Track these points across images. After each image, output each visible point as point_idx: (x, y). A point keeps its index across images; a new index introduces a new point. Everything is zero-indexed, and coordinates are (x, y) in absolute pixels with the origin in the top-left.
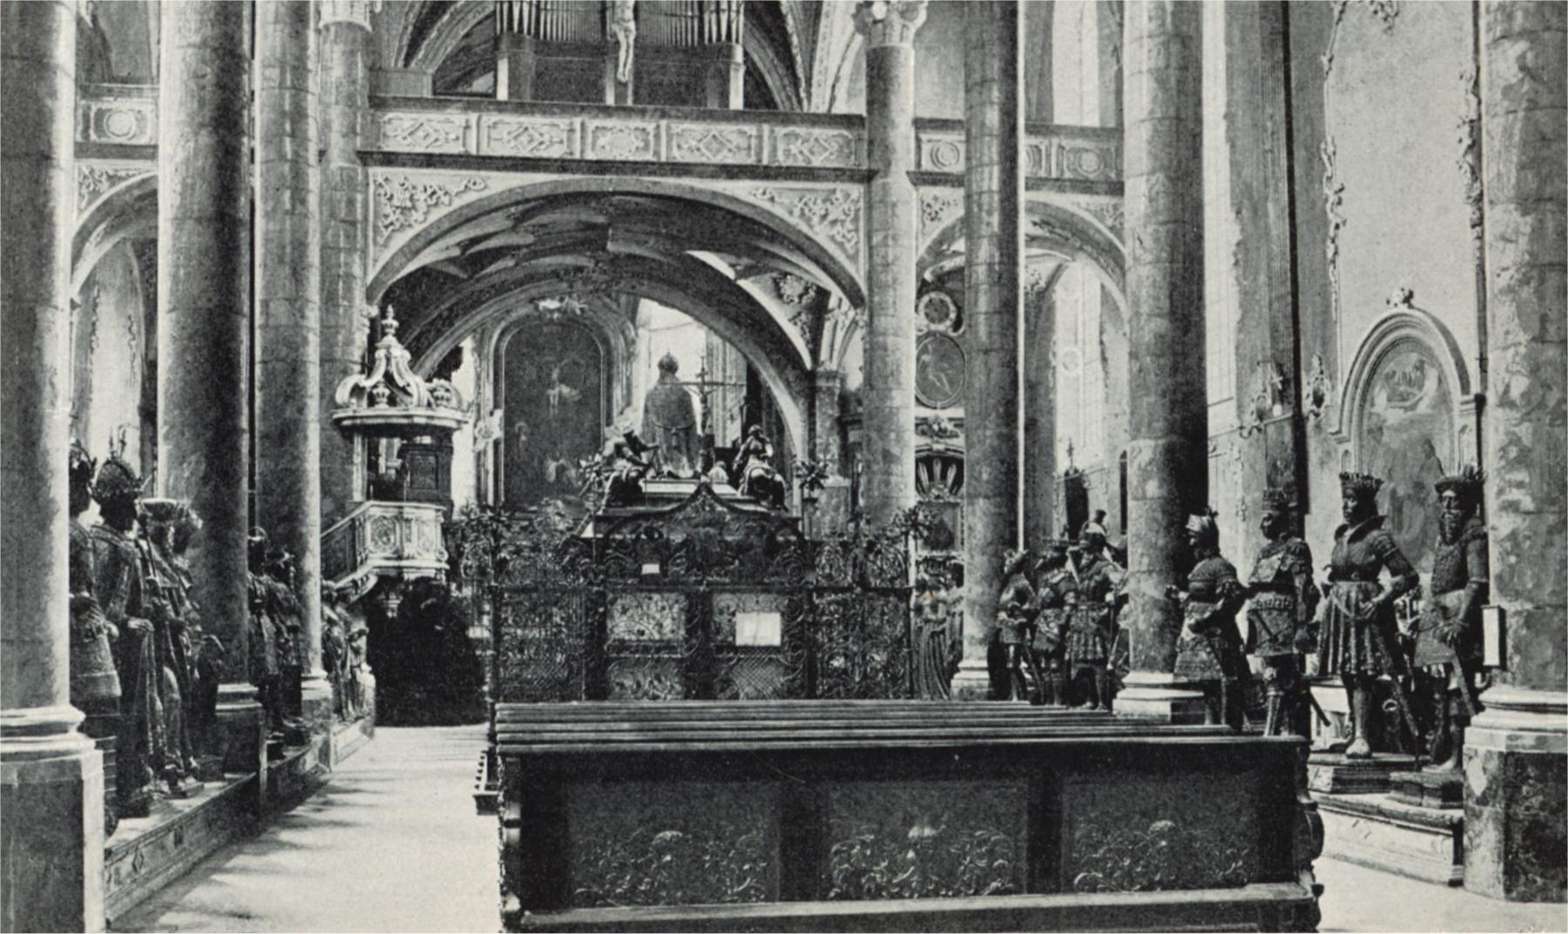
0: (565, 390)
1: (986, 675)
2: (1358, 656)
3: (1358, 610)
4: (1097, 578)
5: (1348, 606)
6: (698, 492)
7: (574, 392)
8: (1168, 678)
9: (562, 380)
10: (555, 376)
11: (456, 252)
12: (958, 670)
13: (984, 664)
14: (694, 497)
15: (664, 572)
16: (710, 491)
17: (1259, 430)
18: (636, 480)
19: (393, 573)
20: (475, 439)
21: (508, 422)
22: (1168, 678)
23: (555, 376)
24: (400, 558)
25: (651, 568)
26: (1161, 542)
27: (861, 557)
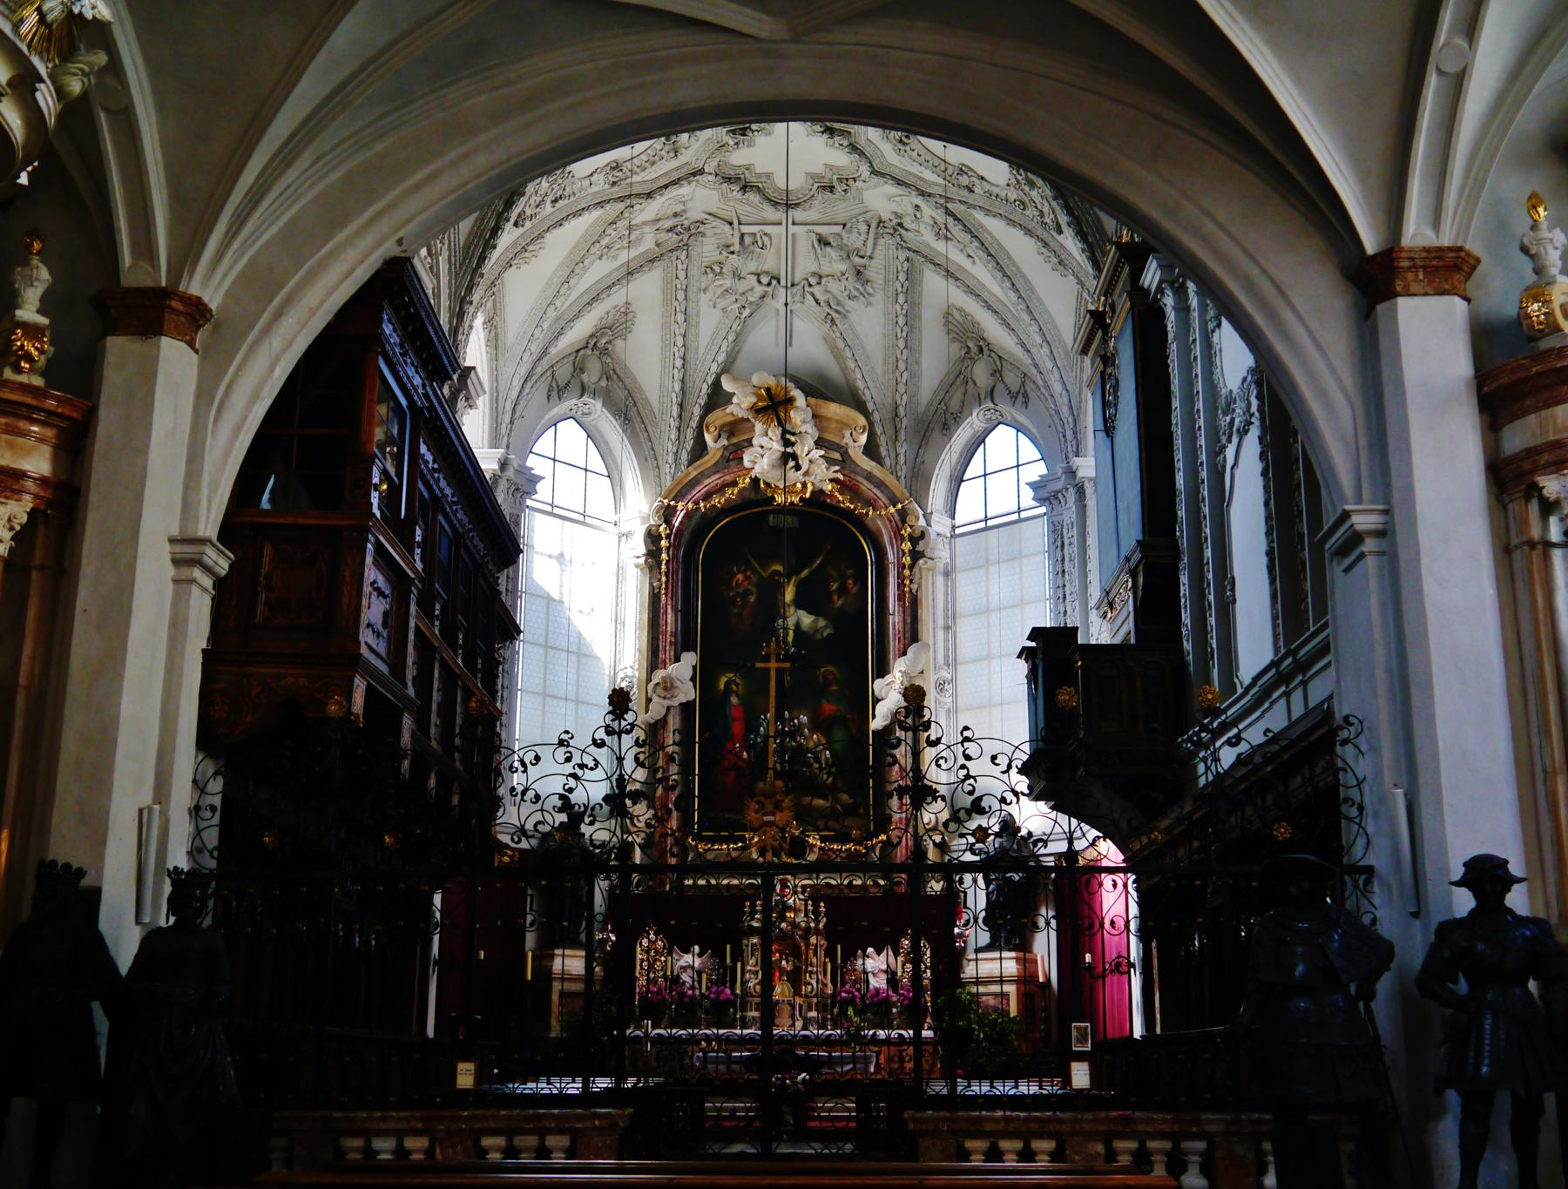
0: (807, 620)
7: (822, 623)
9: (799, 603)
10: (789, 594)
20: (649, 700)
21: (705, 677)
23: (789, 594)
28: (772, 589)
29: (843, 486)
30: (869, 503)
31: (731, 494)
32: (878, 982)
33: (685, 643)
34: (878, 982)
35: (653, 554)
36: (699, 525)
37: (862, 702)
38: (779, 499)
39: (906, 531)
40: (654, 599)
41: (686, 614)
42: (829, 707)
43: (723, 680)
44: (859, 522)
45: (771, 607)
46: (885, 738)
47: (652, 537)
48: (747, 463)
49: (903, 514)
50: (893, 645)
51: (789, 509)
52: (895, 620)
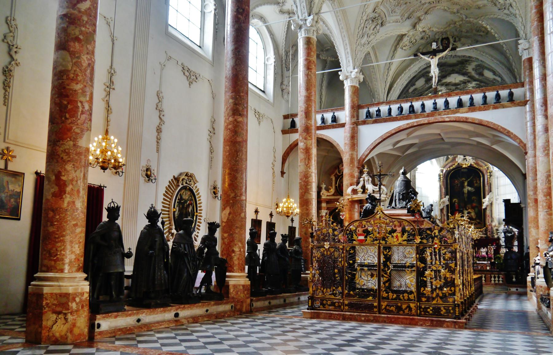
1: (544, 280)
10: (466, 184)
11: (391, 147)
23: (466, 184)
27: (437, 234)
28: (463, 183)
29: (476, 164)
30: (481, 166)
31: (454, 166)
32: (484, 254)
33: (446, 194)
34: (484, 254)
35: (440, 178)
36: (448, 173)
37: (481, 203)
38: (464, 166)
39: (488, 171)
40: (440, 186)
41: (446, 188)
42: (474, 204)
43: (454, 200)
44: (479, 170)
45: (463, 187)
46: (486, 209)
47: (440, 175)
48: (457, 160)
49: (488, 168)
50: (487, 193)
51: (465, 168)
52: (487, 188)
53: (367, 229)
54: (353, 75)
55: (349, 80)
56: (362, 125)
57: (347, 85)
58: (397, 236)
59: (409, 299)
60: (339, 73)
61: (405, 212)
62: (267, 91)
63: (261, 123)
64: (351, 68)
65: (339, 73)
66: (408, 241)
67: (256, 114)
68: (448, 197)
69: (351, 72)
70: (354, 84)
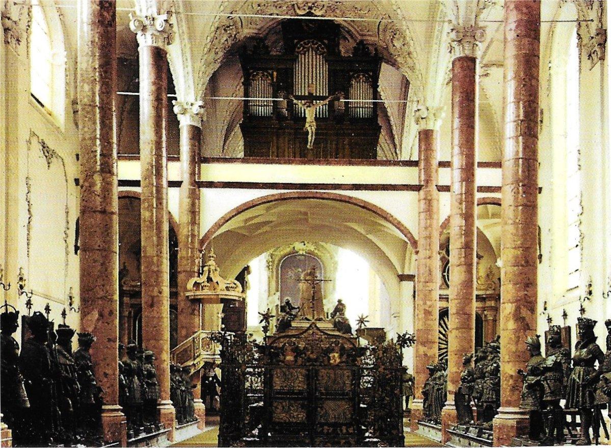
2: (582, 400)
3: (583, 381)
4: (495, 365)
5: (579, 378)
6: (311, 326)
8: (516, 410)
12: (445, 405)
13: (454, 403)
14: (308, 329)
15: (296, 361)
16: (316, 326)
17: (588, 299)
18: (290, 321)
19: (212, 361)
22: (516, 410)
24: (214, 355)
25: (290, 358)
26: (514, 350)
53: (298, 347)
54: (195, 109)
55: (188, 115)
56: (207, 187)
57: (185, 122)
58: (334, 356)
59: (348, 433)
60: (174, 102)
61: (331, 326)
62: (54, 113)
63: (51, 165)
64: (191, 99)
65: (174, 102)
66: (346, 362)
67: (45, 149)
68: (278, 294)
69: (192, 105)
70: (195, 124)
